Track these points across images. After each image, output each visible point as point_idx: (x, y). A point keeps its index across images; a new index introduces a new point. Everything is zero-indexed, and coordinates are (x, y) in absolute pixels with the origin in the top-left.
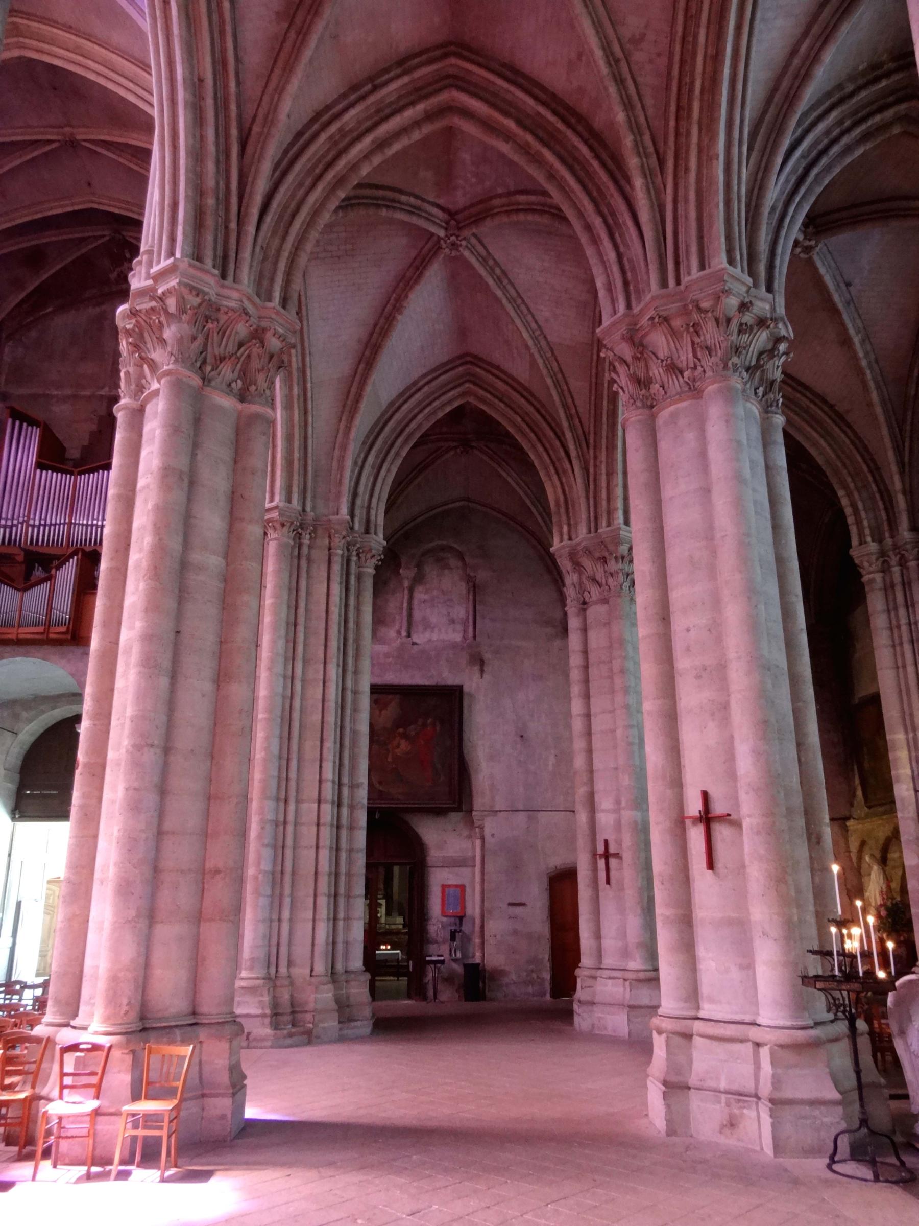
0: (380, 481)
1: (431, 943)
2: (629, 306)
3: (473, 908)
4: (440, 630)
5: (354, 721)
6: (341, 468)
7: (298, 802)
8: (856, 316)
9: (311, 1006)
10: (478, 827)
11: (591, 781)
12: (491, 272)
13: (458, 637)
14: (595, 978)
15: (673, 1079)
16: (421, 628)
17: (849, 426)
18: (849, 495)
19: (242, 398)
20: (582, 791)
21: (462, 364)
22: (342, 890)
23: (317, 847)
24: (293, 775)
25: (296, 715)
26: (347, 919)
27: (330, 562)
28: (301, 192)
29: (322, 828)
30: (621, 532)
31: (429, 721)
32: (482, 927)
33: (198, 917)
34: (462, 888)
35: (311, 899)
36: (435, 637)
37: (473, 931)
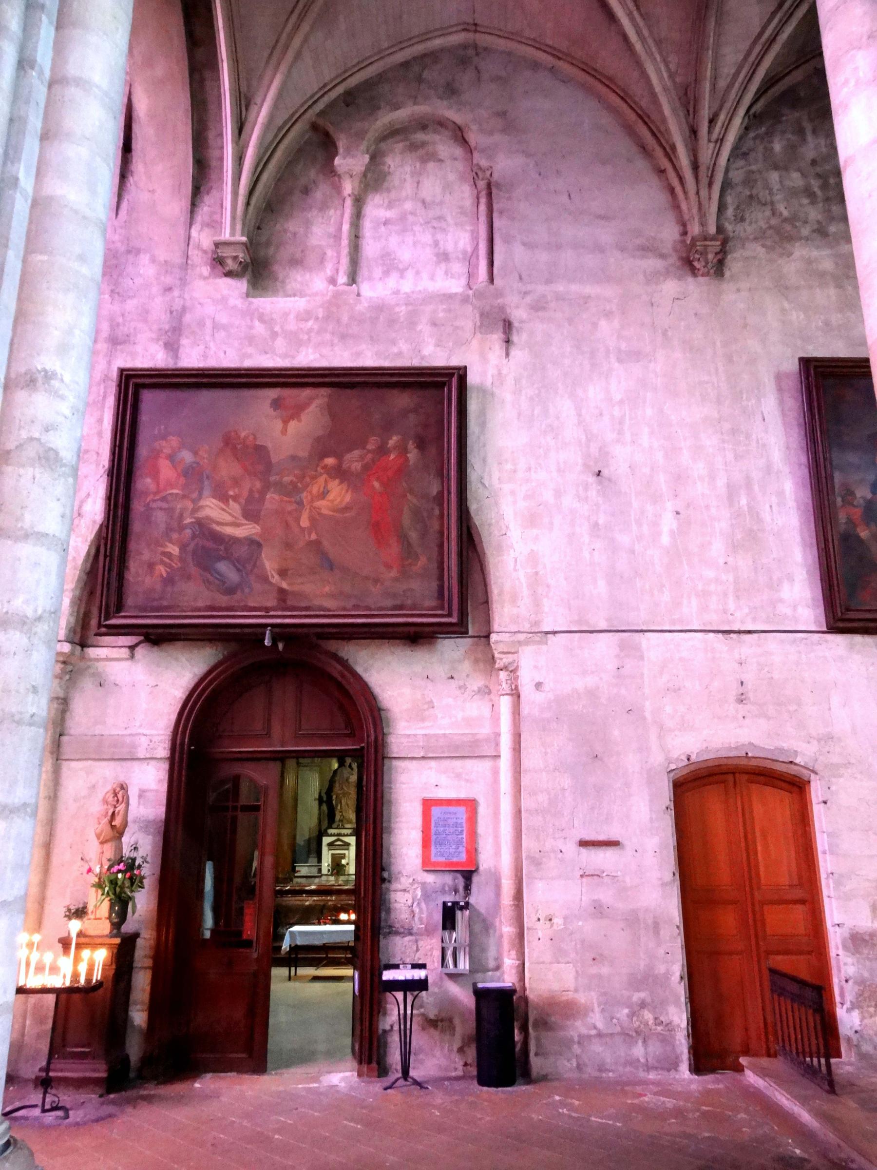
1: (397, 933)
4: (418, 273)
10: (505, 668)
13: (456, 286)
16: (378, 272)
31: (393, 441)
32: (518, 896)
34: (471, 805)
36: (407, 286)
37: (497, 906)
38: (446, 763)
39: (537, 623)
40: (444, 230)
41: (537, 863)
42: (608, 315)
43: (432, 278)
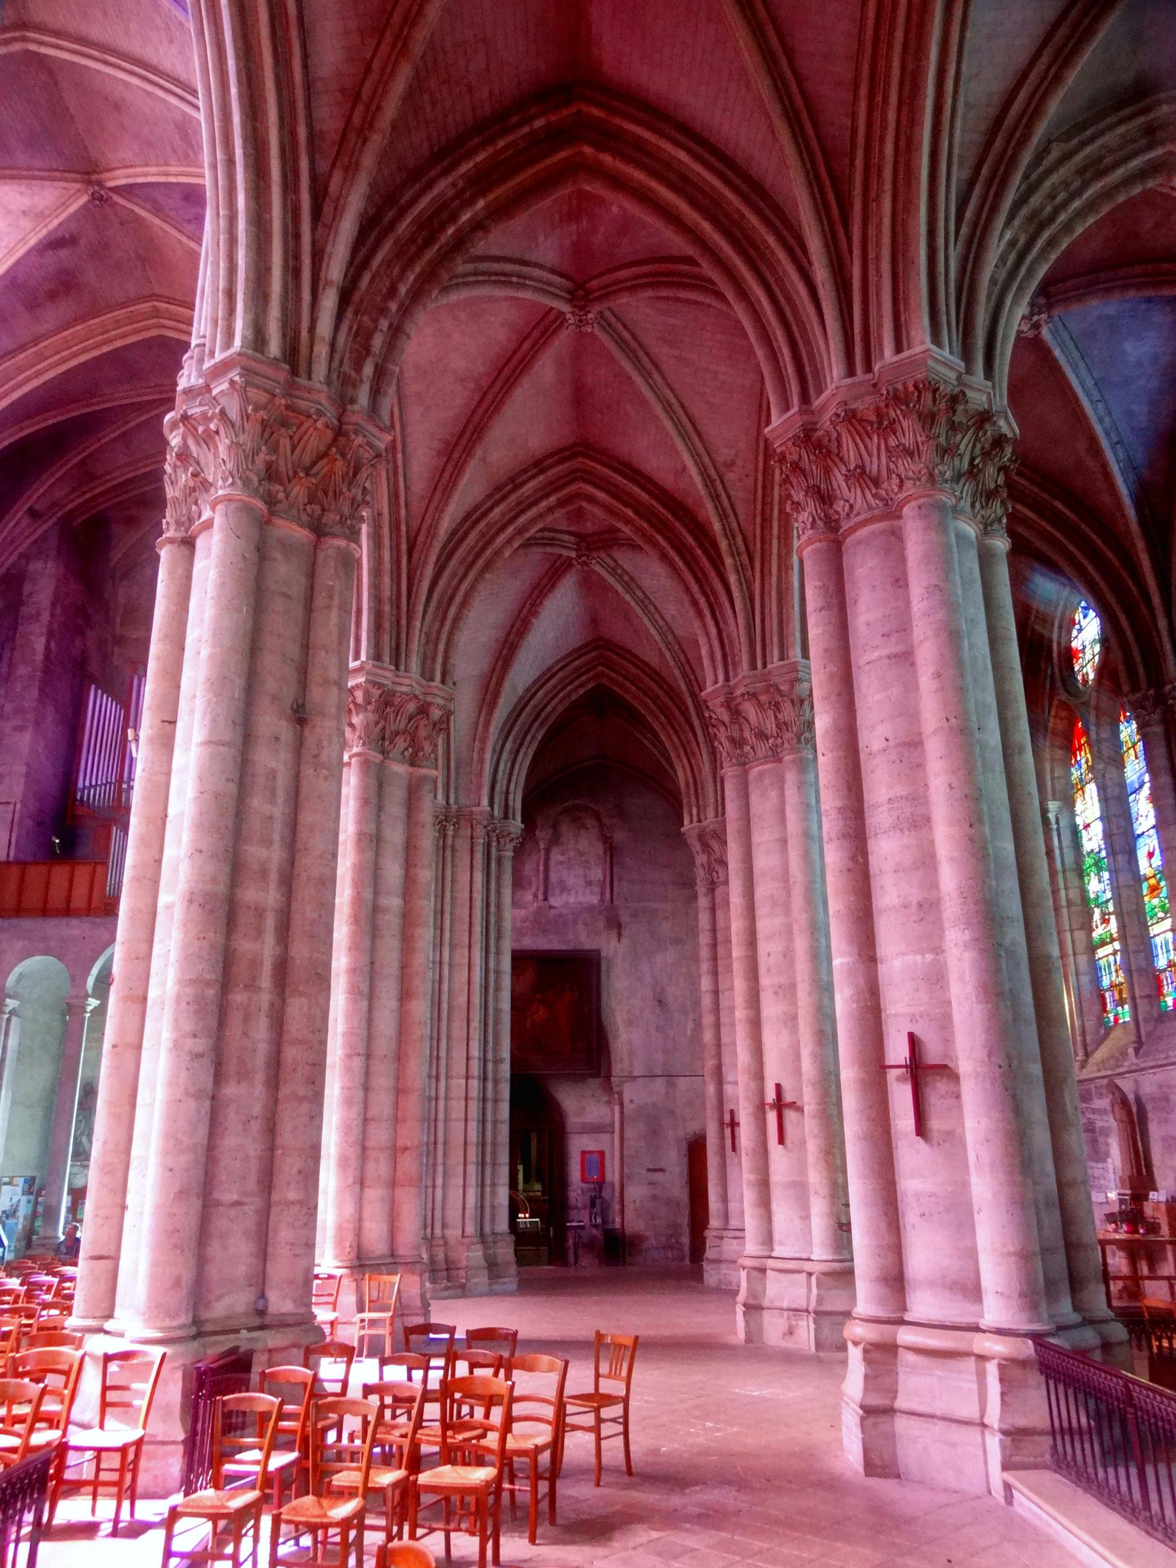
0: (517, 767)
2: (727, 679)
3: (613, 1174)
5: (497, 999)
6: (481, 761)
7: (447, 1078)
9: (464, 1263)
11: (719, 1055)
12: (620, 579)
13: (595, 900)
14: (721, 1238)
15: (752, 1302)
16: (557, 891)
19: (412, 764)
20: (710, 1063)
21: (594, 649)
22: (488, 1159)
23: (466, 1120)
24: (443, 1054)
25: (445, 997)
26: (493, 1185)
27: (472, 851)
28: (456, 580)
29: (470, 1102)
33: (393, 1184)
34: (602, 1154)
35: (461, 1167)
36: (572, 900)
37: (613, 1196)
39: (631, 1072)
41: (629, 1178)
42: (666, 919)
43: (584, 894)
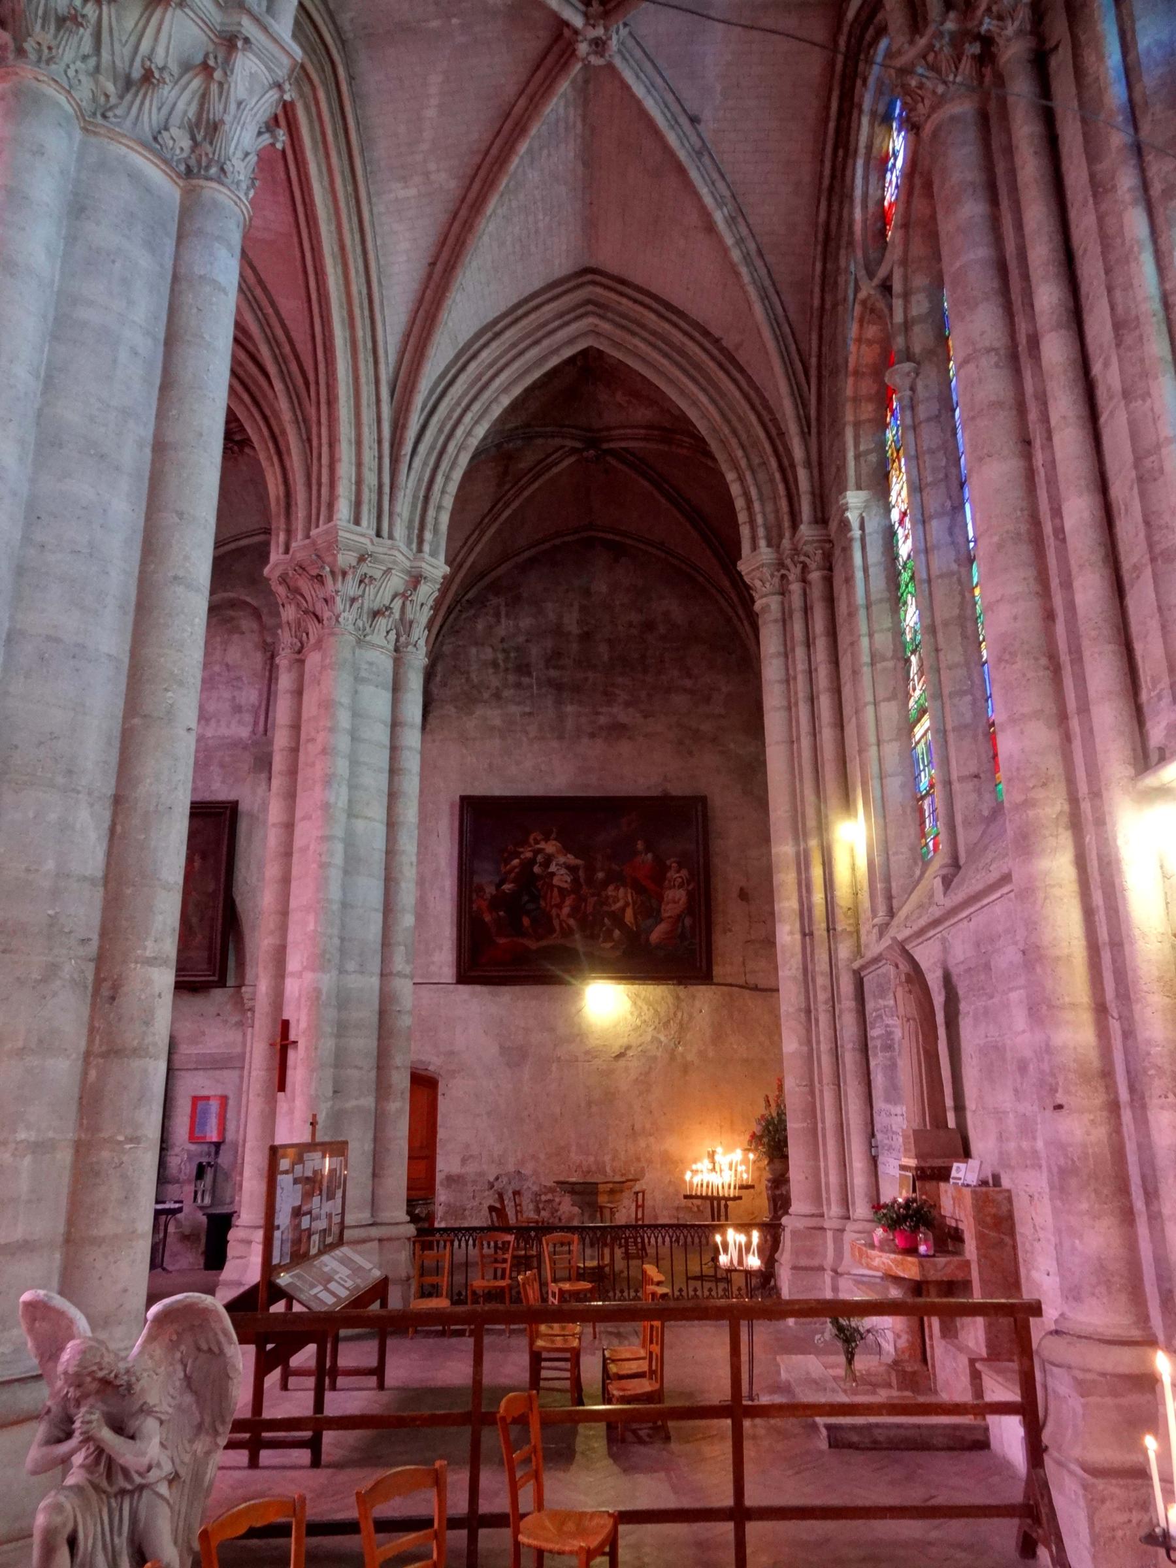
1: (169, 1182)
4: (219, 721)
8: (715, 176)
13: (244, 732)
17: (742, 370)
18: (741, 479)
30: (341, 533)
38: (210, 1073)
40: (240, 689)
43: (228, 726)
